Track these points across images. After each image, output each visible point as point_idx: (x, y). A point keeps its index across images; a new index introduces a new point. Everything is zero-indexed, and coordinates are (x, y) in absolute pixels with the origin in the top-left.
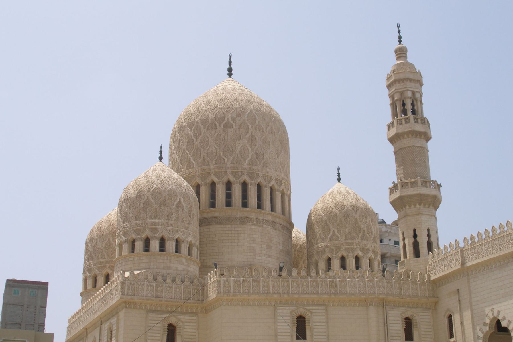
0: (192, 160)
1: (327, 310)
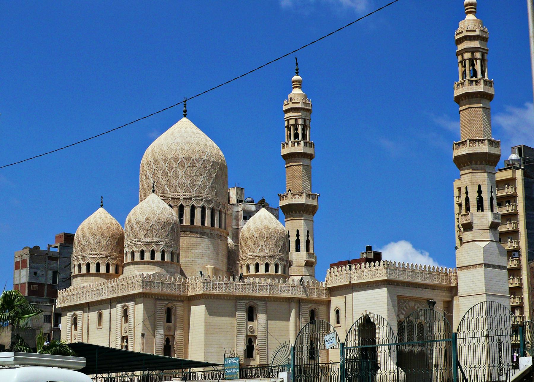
0: (166, 187)
1: (266, 304)
